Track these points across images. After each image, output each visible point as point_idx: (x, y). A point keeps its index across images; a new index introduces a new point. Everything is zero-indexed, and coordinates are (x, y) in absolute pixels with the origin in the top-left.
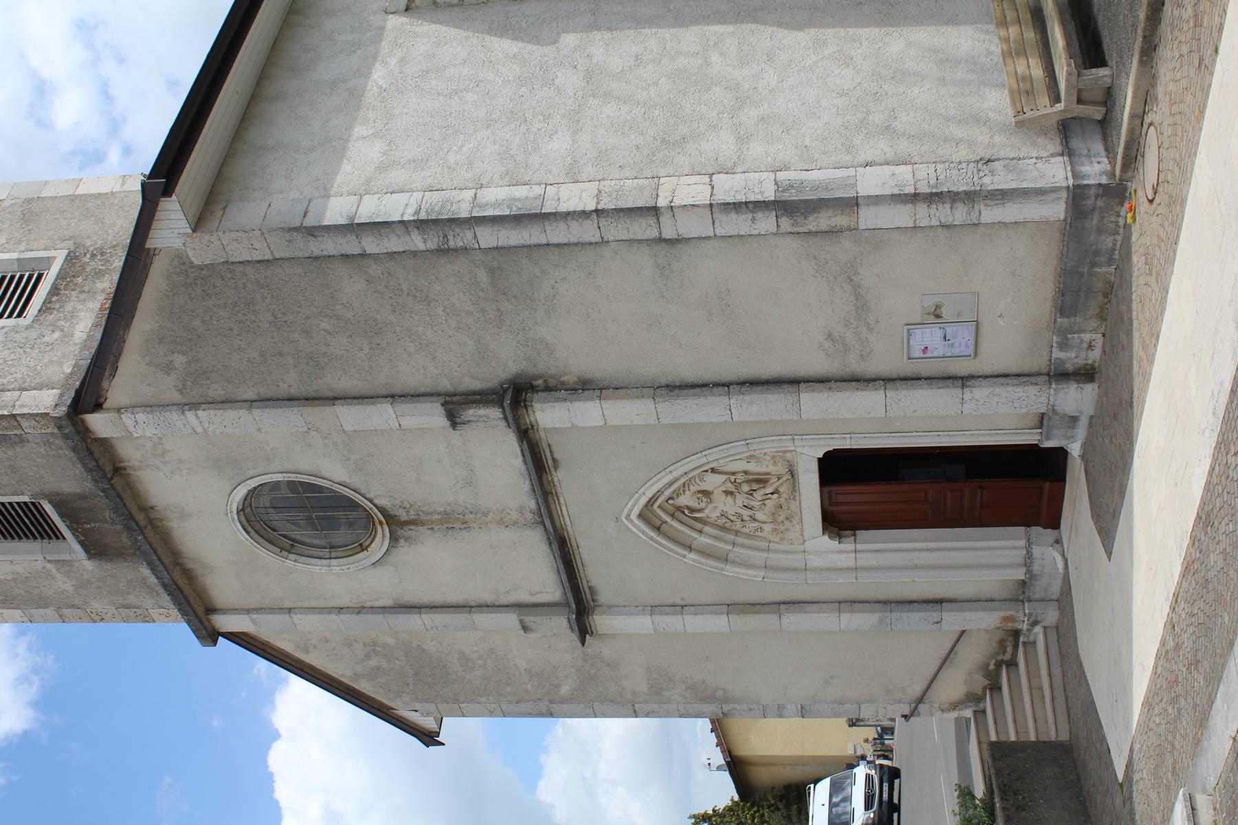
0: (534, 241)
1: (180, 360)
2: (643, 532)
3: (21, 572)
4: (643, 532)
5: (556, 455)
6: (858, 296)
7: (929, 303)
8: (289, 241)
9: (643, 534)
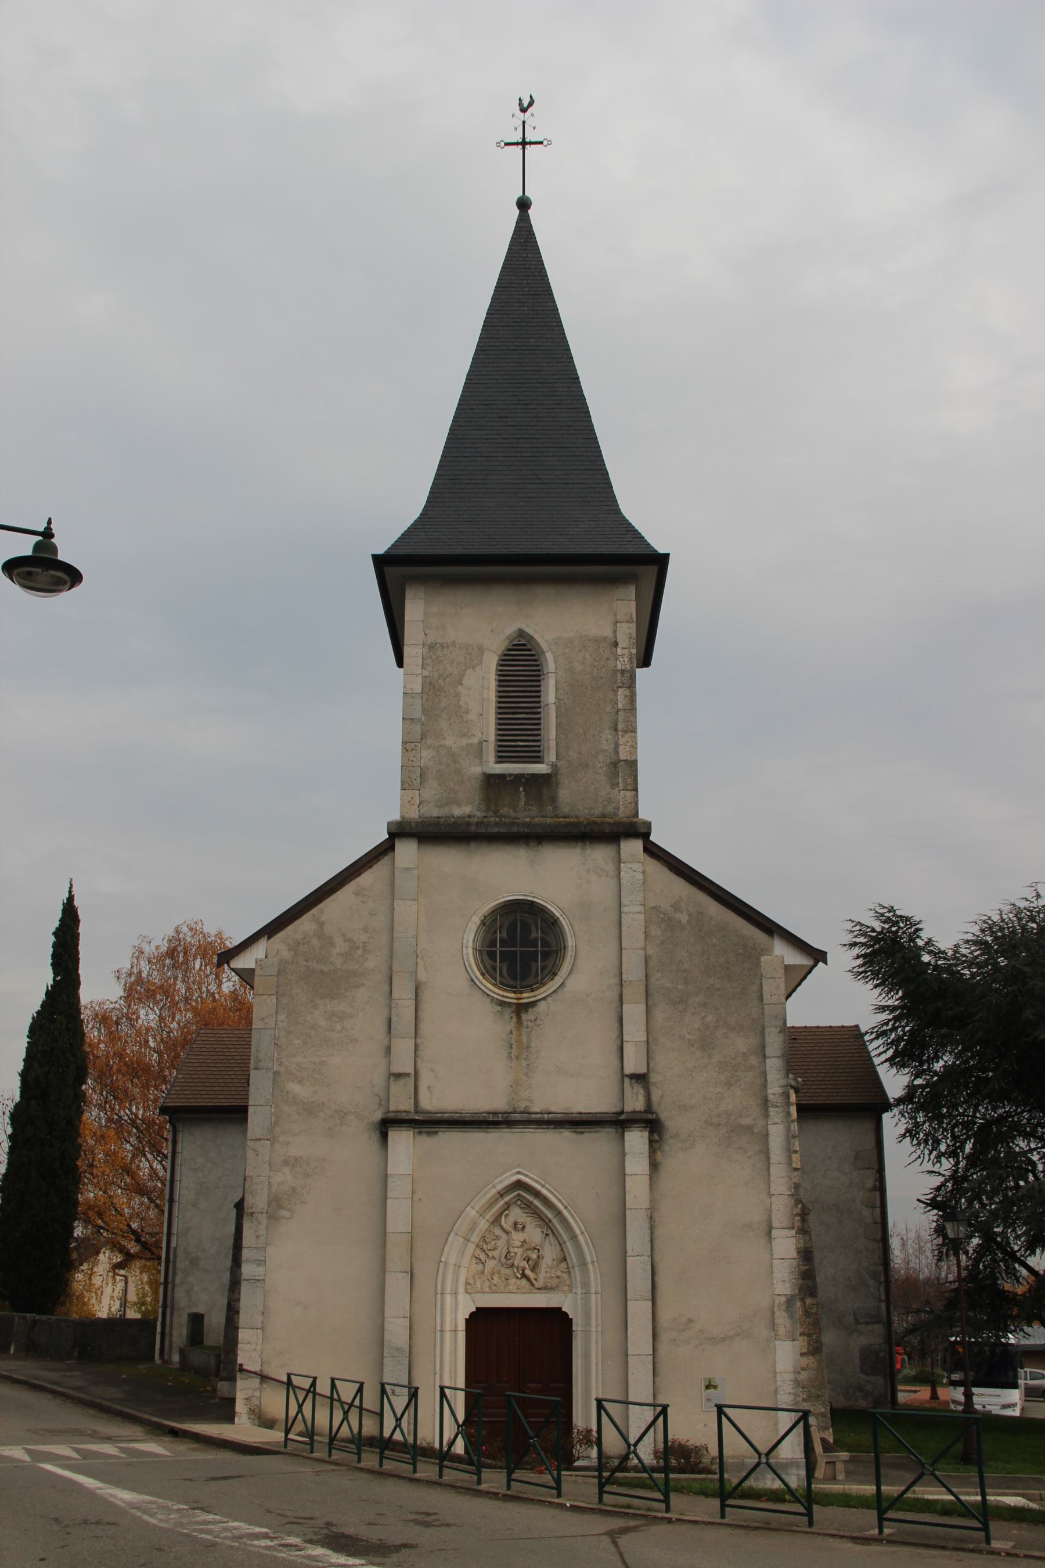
1: (684, 918)
2: (501, 1181)
3: (469, 716)
4: (501, 1181)
5: (586, 1135)
6: (724, 1339)
7: (717, 1382)
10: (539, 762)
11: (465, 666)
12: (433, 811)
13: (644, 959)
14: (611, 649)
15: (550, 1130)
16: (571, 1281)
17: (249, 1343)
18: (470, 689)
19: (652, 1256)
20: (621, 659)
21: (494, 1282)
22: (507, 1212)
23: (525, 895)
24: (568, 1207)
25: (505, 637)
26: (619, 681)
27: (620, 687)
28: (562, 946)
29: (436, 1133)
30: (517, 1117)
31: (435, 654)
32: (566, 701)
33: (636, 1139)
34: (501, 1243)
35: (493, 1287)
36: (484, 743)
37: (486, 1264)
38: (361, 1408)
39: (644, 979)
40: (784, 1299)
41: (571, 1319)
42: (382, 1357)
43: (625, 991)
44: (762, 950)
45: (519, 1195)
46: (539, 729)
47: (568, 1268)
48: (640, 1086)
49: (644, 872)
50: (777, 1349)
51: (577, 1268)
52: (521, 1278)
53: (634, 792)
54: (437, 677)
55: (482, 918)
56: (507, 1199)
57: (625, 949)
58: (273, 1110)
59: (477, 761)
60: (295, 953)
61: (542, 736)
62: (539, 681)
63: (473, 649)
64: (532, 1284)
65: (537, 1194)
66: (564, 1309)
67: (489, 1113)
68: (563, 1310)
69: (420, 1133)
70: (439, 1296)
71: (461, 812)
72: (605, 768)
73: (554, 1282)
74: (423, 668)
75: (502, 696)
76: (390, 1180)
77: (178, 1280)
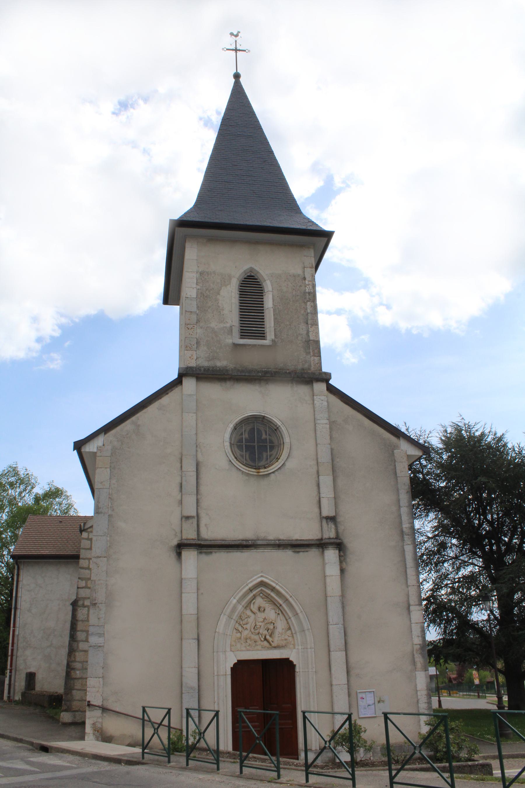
0: (408, 563)
2: (252, 582)
4: (252, 582)
5: (301, 553)
8: (404, 484)
10: (264, 339)
11: (221, 285)
12: (205, 363)
13: (330, 451)
14: (302, 281)
15: (281, 550)
17: (94, 687)
18: (224, 297)
19: (344, 625)
20: (308, 287)
22: (254, 601)
23: (260, 413)
24: (293, 596)
25: (243, 271)
26: (307, 298)
27: (308, 301)
28: (282, 443)
29: (211, 553)
30: (259, 542)
31: (204, 277)
32: (279, 307)
33: (331, 554)
34: (251, 620)
36: (233, 327)
38: (169, 727)
39: (331, 461)
40: (419, 647)
42: (182, 693)
43: (320, 469)
44: (394, 446)
45: (261, 590)
46: (263, 322)
47: (292, 634)
48: (332, 523)
49: (328, 402)
50: (417, 676)
51: (298, 634)
52: (264, 640)
53: (318, 358)
54: (205, 290)
55: (235, 425)
57: (319, 444)
58: (108, 539)
59: (229, 336)
60: (122, 443)
61: (265, 325)
62: (262, 296)
63: (225, 276)
64: (270, 644)
65: (273, 589)
66: (291, 659)
67: (243, 540)
69: (201, 553)
71: (221, 365)
72: (302, 344)
73: (284, 643)
74: (197, 284)
75: (242, 303)
76: (184, 582)
77: (19, 654)
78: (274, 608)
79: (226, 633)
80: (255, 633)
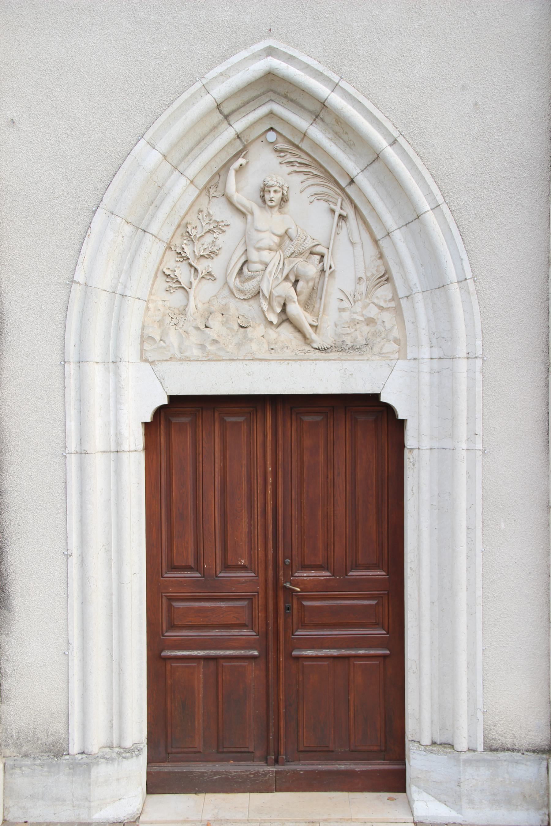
2: (224, 75)
4: (224, 75)
9: (221, 74)
16: (403, 328)
21: (212, 334)
22: (241, 161)
24: (401, 140)
35: (210, 348)
37: (192, 292)
41: (402, 422)
45: (271, 114)
47: (395, 298)
51: (419, 297)
52: (279, 325)
56: (240, 125)
68: (383, 399)
70: (71, 369)
78: (324, 194)
79: (119, 290)
80: (242, 292)
